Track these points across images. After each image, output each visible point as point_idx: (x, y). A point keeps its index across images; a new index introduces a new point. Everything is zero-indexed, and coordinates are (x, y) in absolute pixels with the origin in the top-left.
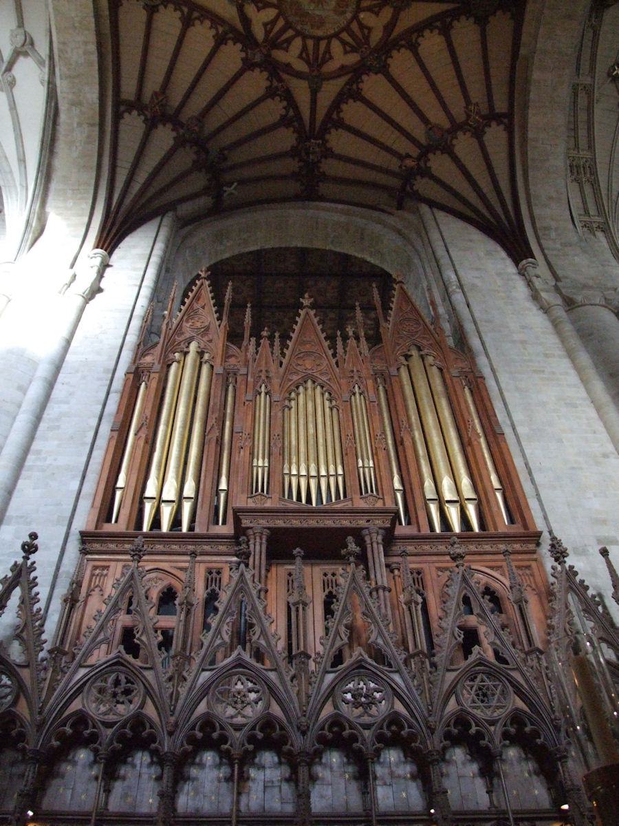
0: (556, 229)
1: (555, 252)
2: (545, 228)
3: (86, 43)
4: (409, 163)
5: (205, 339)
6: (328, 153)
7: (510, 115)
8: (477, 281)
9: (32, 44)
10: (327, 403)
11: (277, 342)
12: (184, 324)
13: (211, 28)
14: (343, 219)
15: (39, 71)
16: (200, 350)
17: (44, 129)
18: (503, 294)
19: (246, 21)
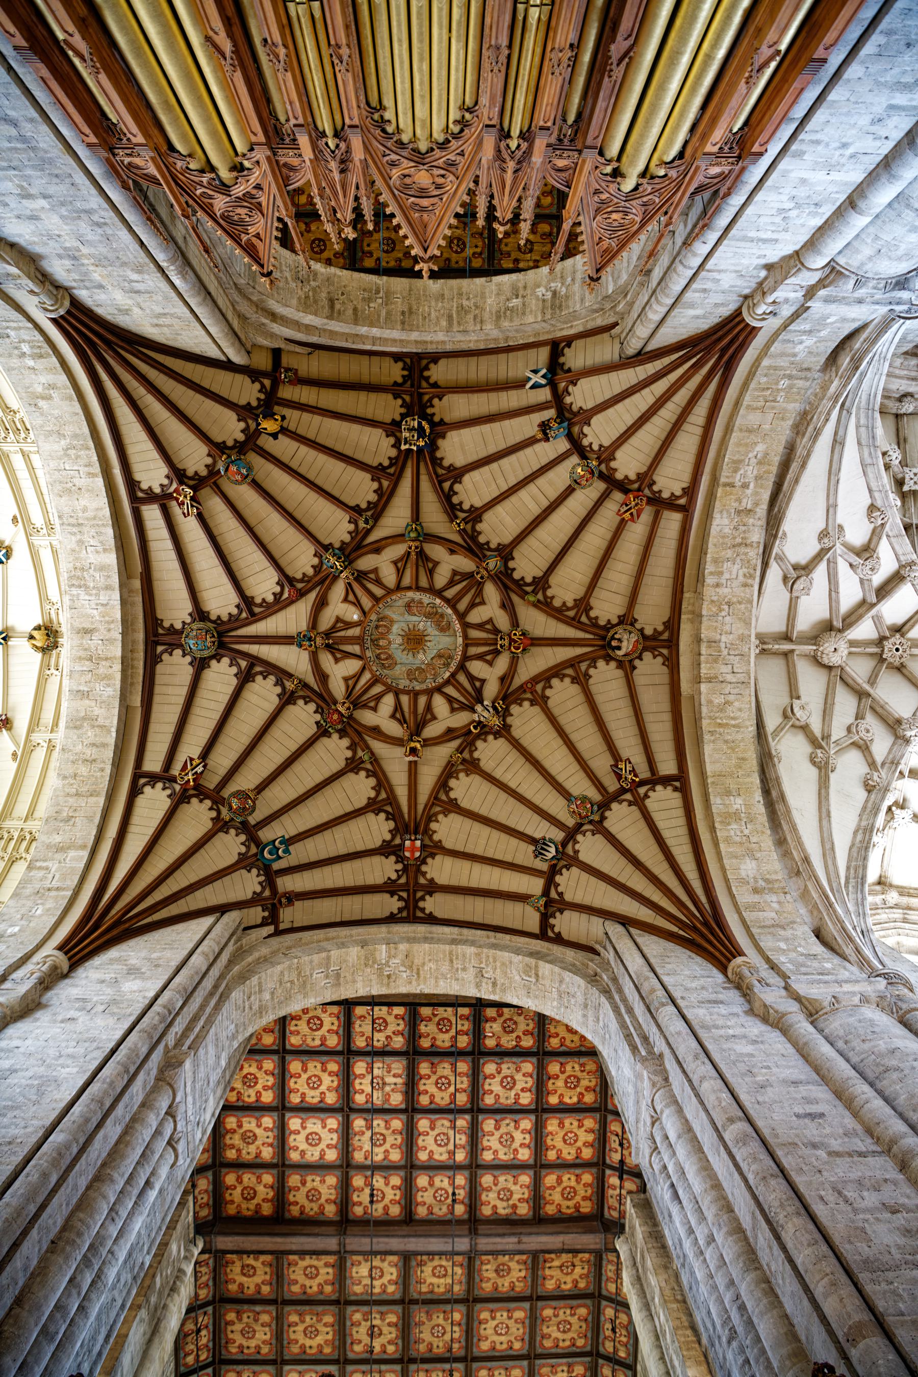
0: (23, 354)
1: (15, 325)
2: (41, 356)
3: (718, 585)
4: (269, 425)
5: (604, 196)
6: (392, 428)
7: (136, 501)
8: (135, 277)
9: (785, 579)
10: (389, 115)
11: (481, 211)
12: (638, 219)
13: (553, 598)
14: (363, 330)
15: (785, 549)
16: (619, 179)
17: (797, 481)
18: (86, 261)
19: (507, 606)
